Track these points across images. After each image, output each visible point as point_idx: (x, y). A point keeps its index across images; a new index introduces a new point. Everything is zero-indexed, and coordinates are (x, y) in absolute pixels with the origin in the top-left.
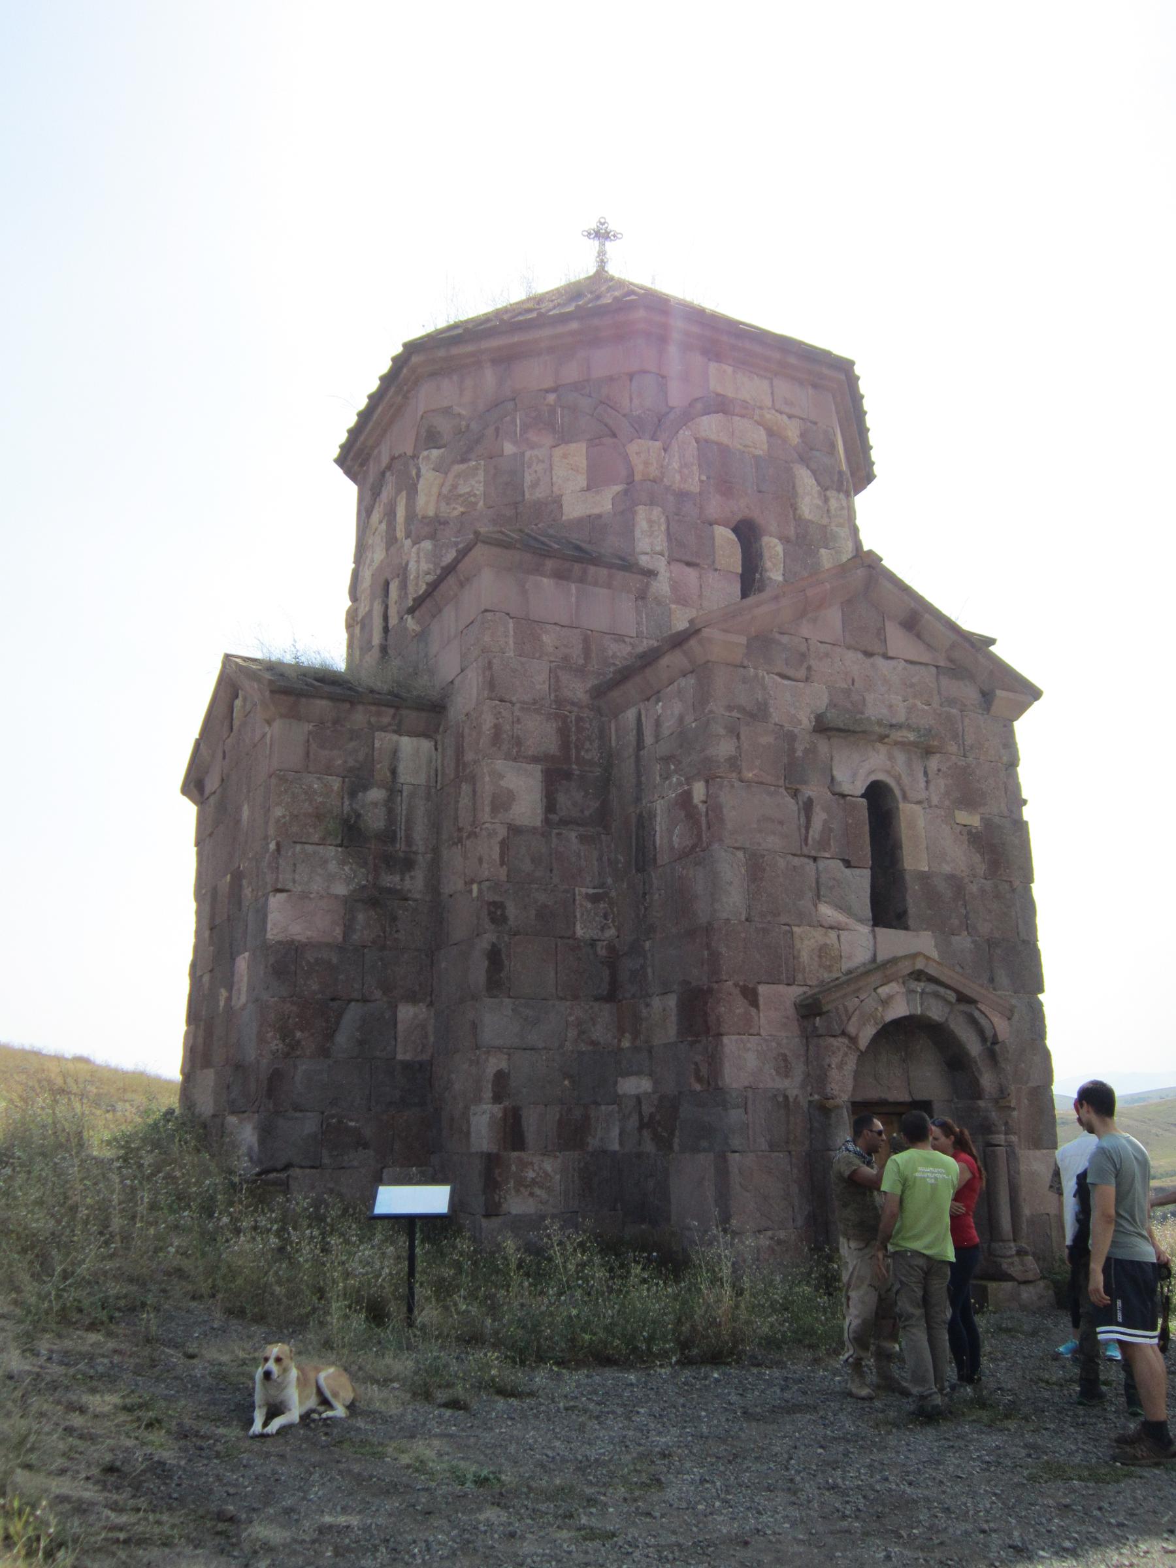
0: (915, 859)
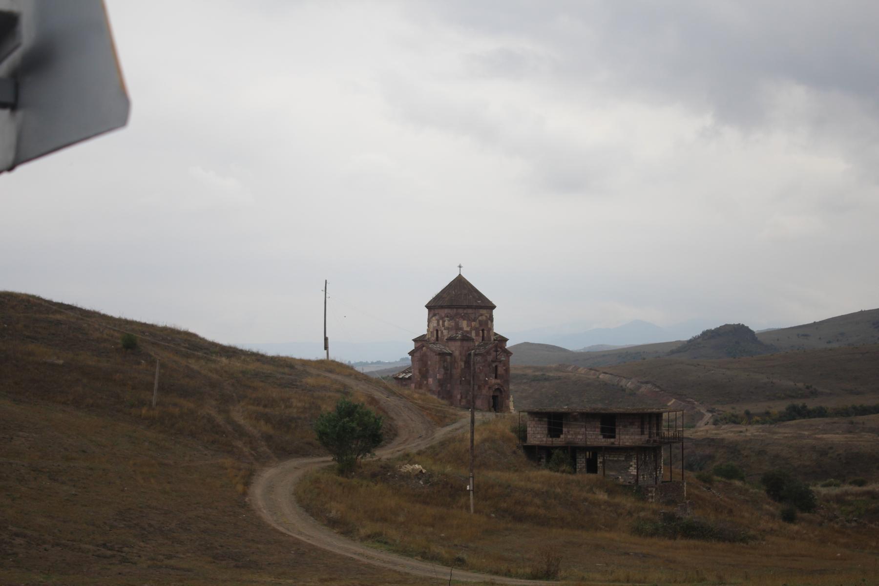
0: (499, 373)
